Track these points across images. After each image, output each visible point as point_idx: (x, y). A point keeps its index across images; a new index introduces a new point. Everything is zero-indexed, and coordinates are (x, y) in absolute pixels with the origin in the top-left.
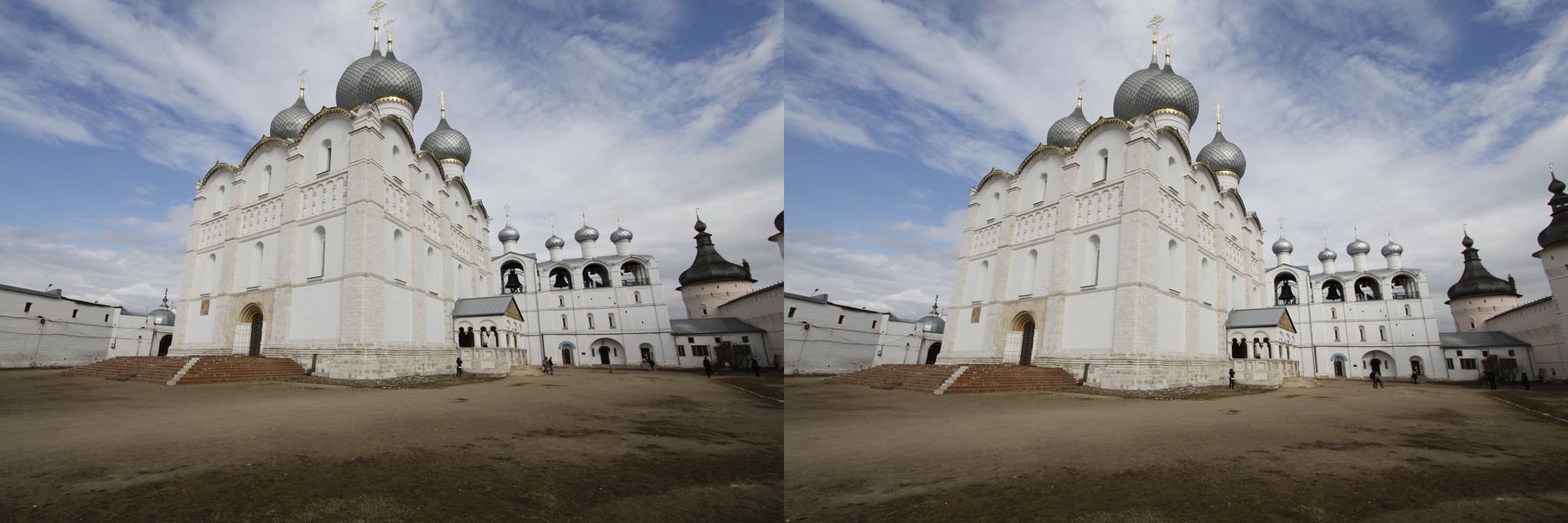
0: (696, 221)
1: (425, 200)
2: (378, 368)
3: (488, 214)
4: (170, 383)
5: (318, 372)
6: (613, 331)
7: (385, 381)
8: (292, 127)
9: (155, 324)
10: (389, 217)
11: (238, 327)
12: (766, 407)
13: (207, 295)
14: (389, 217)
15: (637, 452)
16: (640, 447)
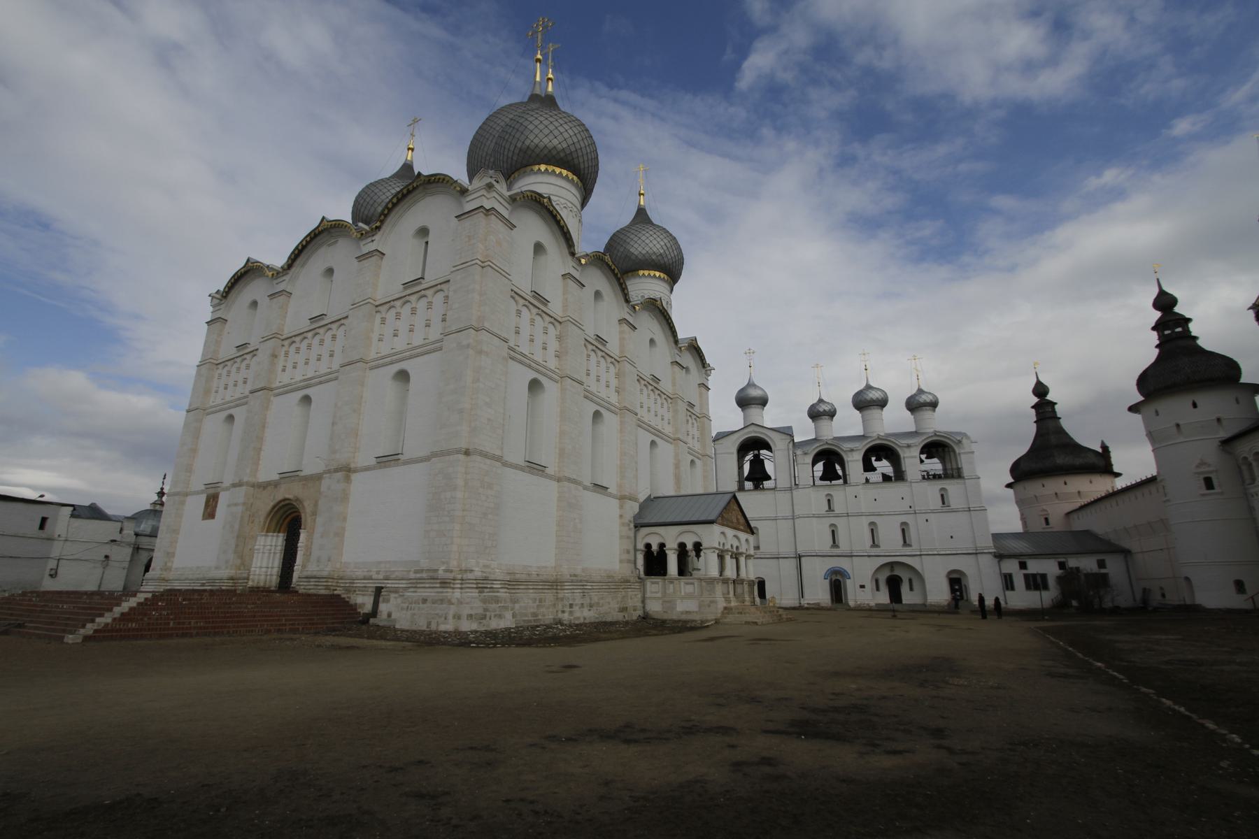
0: (1035, 381)
1: (591, 333)
6: (907, 551)
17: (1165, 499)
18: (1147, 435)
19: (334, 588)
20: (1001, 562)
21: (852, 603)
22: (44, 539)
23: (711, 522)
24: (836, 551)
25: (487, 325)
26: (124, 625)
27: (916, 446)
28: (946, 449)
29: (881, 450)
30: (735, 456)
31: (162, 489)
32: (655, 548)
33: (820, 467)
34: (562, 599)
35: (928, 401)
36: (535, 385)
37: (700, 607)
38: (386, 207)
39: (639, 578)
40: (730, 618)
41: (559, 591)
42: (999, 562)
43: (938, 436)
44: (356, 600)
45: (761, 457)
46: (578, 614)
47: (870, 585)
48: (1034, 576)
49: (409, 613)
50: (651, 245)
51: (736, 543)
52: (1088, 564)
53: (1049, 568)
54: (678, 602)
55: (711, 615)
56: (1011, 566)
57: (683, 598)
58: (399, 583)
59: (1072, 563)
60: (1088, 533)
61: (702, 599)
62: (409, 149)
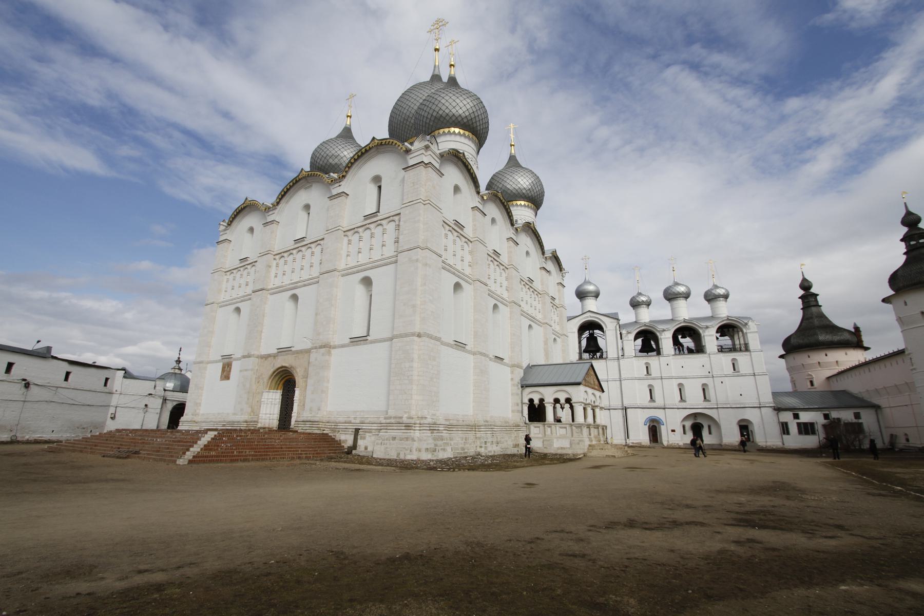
2: (432, 446)
3: (564, 265)
4: (181, 462)
5: (360, 450)
7: (440, 461)
8: (336, 160)
9: (165, 390)
10: (448, 268)
11: (265, 395)
12: (880, 495)
13: (229, 356)
14: (448, 268)
15: (733, 547)
16: (737, 542)
17: (912, 368)
18: (897, 320)
19: (324, 429)
20: (779, 413)
21: (665, 443)
22: (106, 393)
23: (579, 384)
24: (653, 405)
25: (429, 246)
26: (208, 453)
27: (713, 327)
28: (735, 330)
30: (576, 335)
31: (179, 358)
32: (536, 402)
33: (639, 341)
34: (480, 438)
35: (722, 294)
36: (457, 286)
37: (571, 444)
38: (350, 162)
39: (525, 423)
40: (594, 453)
41: (477, 432)
42: (777, 414)
43: (730, 320)
44: (340, 437)
45: (595, 335)
46: (490, 449)
47: (679, 430)
48: (805, 424)
50: (522, 182)
51: (593, 399)
52: (847, 416)
54: (555, 440)
55: (580, 450)
56: (787, 417)
57: (558, 438)
58: (372, 426)
59: (834, 414)
60: (844, 392)
61: (573, 439)
62: (348, 116)
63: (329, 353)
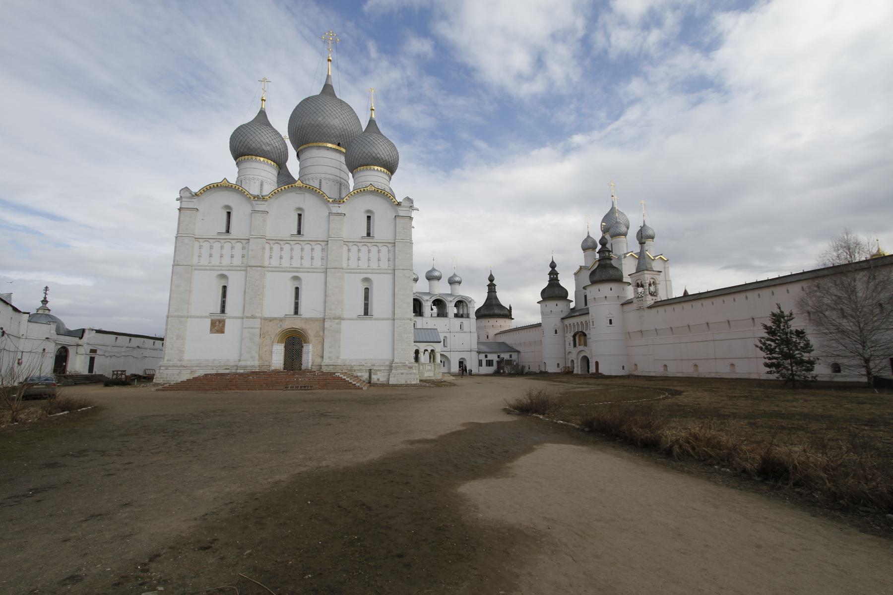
6: (445, 349)
29: (439, 303)
31: (45, 298)
37: (434, 374)
48: (489, 360)
49: (395, 378)
52: (506, 356)
53: (494, 357)
56: (482, 357)
57: (427, 371)
59: (502, 356)
60: (503, 343)
63: (339, 324)
